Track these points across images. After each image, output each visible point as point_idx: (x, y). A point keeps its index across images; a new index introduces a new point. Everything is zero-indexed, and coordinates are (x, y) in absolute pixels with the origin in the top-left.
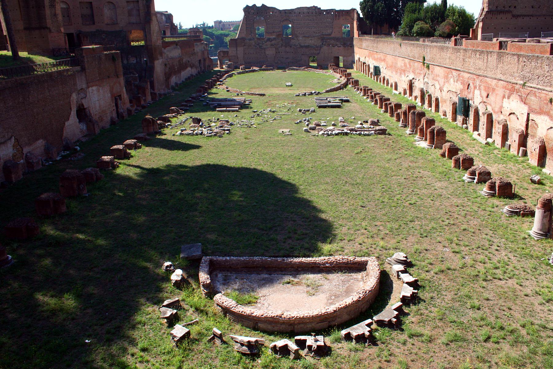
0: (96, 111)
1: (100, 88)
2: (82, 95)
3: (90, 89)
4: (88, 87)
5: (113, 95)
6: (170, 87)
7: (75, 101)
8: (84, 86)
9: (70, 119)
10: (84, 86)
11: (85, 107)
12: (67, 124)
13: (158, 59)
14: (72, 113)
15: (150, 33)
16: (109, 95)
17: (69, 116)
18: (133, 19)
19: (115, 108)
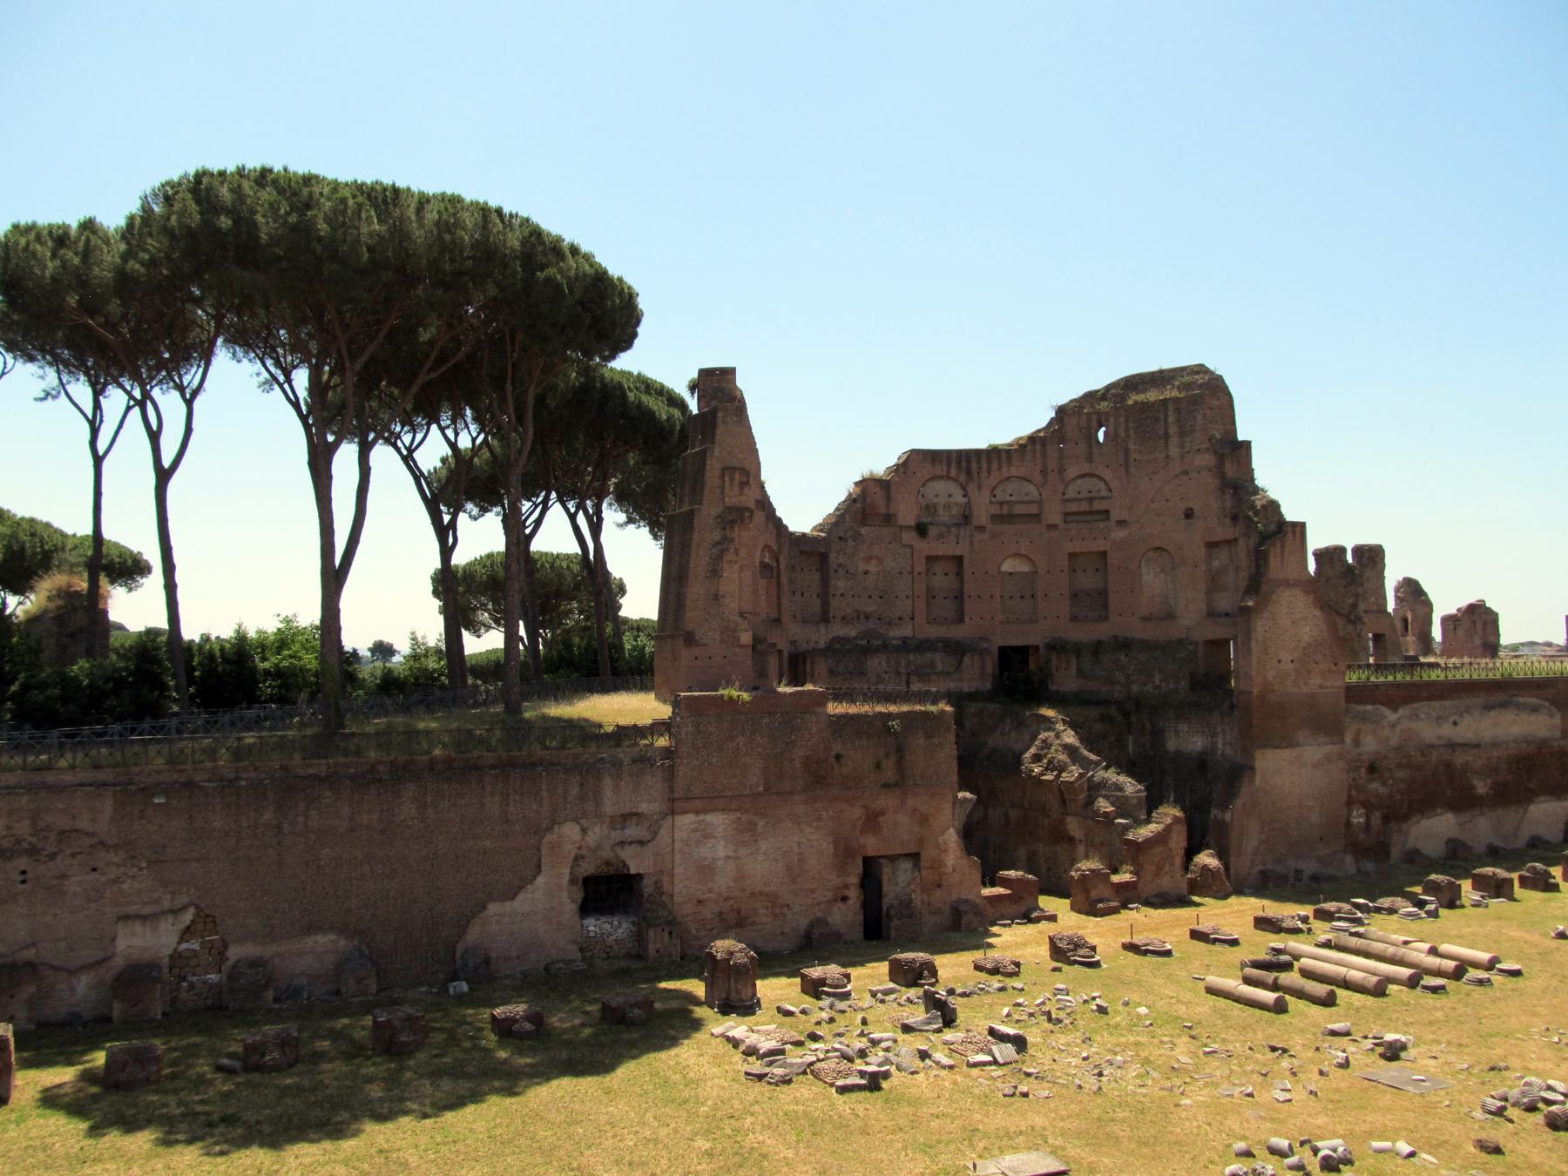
0: (710, 891)
1: (761, 823)
2: (633, 832)
3: (686, 821)
4: (673, 813)
5: (845, 851)
6: (1395, 853)
7: (570, 849)
8: (644, 807)
9: (520, 897)
10: (649, 805)
11: (633, 871)
12: (492, 908)
13: (1292, 744)
14: (540, 880)
15: (1249, 650)
16: (827, 848)
17: (521, 888)
18: (1224, 602)
19: (854, 894)
